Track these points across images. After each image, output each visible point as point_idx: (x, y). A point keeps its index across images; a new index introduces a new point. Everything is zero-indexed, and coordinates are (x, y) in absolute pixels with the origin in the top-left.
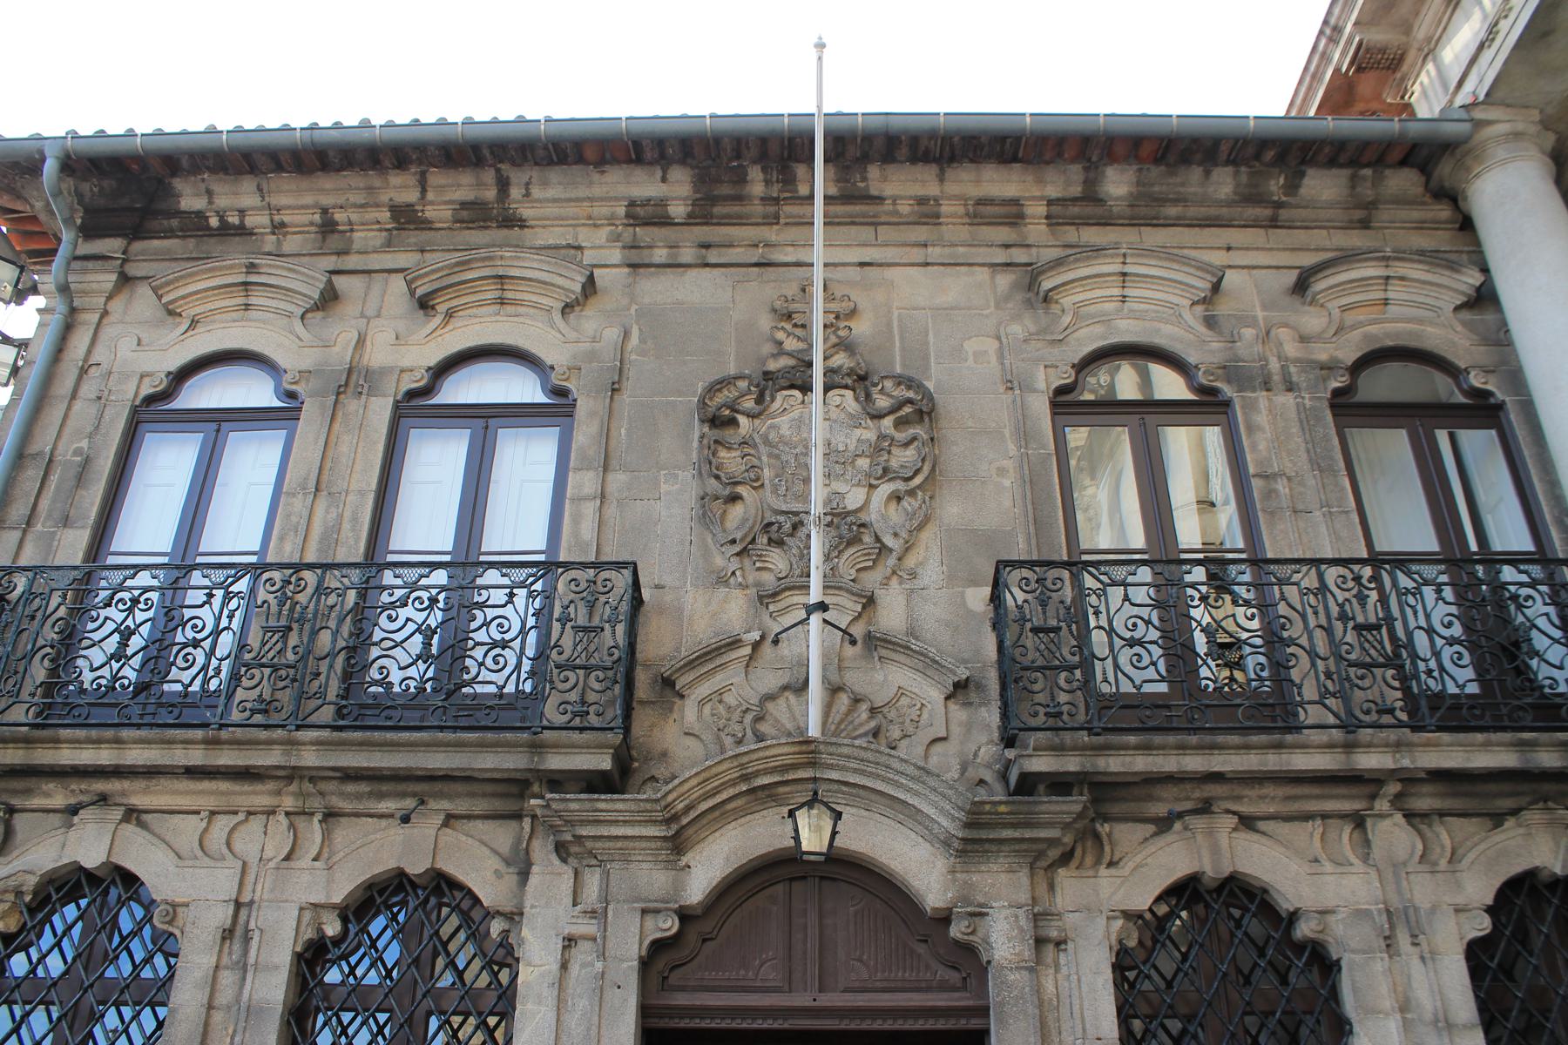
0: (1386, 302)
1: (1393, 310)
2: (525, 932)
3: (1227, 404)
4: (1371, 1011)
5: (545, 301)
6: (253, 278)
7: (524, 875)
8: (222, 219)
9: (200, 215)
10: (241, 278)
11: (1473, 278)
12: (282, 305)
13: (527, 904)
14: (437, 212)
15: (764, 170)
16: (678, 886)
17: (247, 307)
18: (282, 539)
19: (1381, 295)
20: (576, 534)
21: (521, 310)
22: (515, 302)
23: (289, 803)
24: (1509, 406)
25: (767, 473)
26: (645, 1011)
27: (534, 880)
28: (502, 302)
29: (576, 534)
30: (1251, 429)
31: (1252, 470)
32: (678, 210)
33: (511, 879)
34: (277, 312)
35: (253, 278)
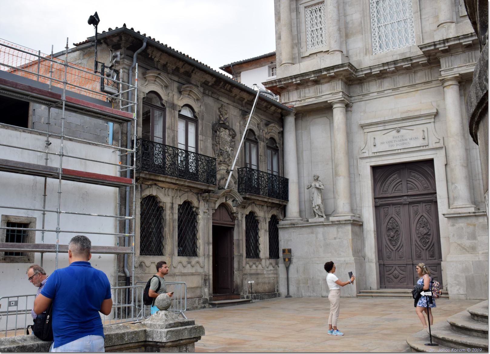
0: (272, 129)
1: (273, 131)
2: (200, 211)
3: (258, 142)
4: (261, 228)
5: (195, 97)
6: (159, 76)
7: (199, 202)
8: (151, 57)
9: (149, 54)
10: (157, 75)
11: (281, 129)
12: (161, 83)
13: (200, 206)
14: (182, 70)
15: (224, 83)
16: (215, 206)
17: (155, 81)
18: (168, 138)
19: (272, 128)
20: (200, 147)
21: (191, 97)
22: (191, 96)
23: (176, 188)
24: (280, 150)
25: (221, 142)
26: (213, 223)
27: (200, 203)
28: (189, 95)
29: (200, 147)
30: (260, 147)
31: (259, 154)
32: (210, 84)
33: (198, 203)
34: (159, 84)
35: (159, 76)
